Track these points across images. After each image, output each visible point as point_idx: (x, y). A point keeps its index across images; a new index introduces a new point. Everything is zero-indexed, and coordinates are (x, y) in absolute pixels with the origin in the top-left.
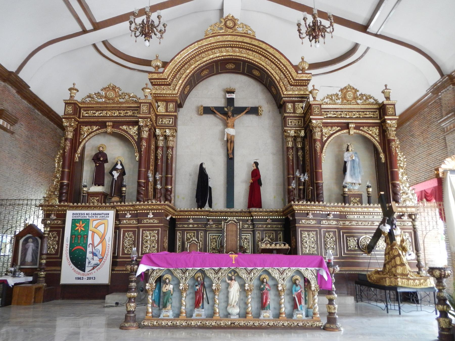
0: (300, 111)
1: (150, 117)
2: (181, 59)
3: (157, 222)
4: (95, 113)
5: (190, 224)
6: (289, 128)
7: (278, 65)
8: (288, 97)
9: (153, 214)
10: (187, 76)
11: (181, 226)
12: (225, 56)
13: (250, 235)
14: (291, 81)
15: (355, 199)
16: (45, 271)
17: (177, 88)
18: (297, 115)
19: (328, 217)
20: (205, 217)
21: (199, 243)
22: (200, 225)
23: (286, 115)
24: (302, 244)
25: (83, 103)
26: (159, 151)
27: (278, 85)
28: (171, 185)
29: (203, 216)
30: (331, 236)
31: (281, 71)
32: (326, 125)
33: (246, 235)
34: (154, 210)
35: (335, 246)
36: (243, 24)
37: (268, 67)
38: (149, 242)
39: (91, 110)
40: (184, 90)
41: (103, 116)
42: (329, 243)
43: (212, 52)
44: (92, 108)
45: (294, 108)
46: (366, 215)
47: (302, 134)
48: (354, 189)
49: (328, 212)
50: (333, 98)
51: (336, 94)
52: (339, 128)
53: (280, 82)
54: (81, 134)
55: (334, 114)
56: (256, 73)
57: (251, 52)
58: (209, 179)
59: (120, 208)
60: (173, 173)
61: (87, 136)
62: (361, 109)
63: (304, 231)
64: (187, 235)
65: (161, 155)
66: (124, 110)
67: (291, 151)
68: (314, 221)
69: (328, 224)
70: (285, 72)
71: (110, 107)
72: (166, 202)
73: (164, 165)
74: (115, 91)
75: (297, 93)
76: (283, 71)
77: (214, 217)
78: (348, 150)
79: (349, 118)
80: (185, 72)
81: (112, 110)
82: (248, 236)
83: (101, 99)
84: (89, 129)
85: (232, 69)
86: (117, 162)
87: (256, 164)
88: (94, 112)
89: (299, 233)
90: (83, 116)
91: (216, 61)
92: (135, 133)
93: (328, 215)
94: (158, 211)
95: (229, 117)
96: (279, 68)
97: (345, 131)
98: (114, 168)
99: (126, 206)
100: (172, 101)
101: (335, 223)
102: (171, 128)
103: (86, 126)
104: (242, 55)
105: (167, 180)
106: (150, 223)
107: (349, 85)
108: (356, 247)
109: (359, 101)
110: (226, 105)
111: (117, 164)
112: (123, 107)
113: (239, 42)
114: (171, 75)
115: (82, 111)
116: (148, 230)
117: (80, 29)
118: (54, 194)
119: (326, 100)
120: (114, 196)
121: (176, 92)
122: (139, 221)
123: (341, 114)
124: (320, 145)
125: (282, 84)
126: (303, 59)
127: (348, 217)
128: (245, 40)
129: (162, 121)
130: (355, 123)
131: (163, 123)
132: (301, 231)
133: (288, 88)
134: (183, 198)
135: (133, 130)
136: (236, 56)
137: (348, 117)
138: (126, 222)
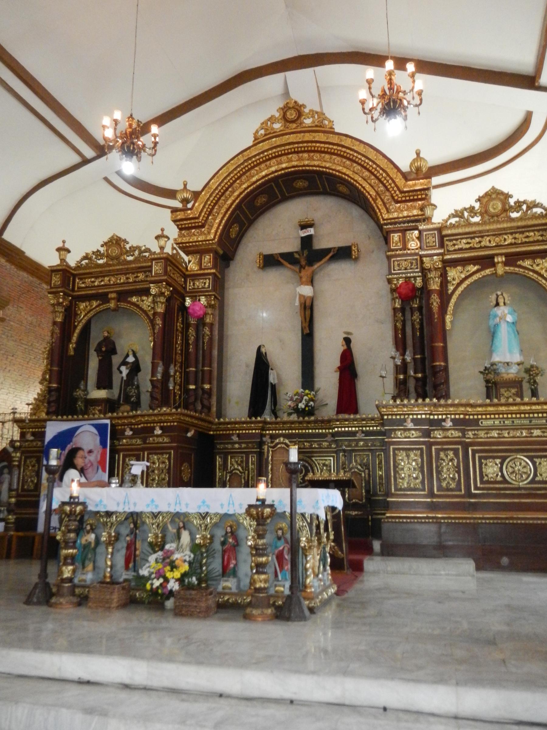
1: (166, 279)
2: (218, 183)
3: (168, 441)
4: (94, 282)
5: (236, 443)
6: (395, 276)
7: (373, 170)
8: (391, 224)
9: (161, 428)
10: (228, 210)
11: (222, 446)
12: (287, 168)
13: (332, 459)
14: (397, 195)
15: (508, 390)
16: (15, 514)
17: (213, 231)
18: (409, 252)
19: (443, 424)
20: (257, 431)
21: (244, 473)
22: (250, 445)
23: (390, 253)
24: (395, 472)
25: (79, 267)
27: (374, 205)
28: (210, 383)
29: (255, 429)
30: (449, 457)
31: (380, 180)
33: (326, 460)
34: (164, 422)
35: (457, 475)
36: (313, 111)
37: (357, 177)
38: (156, 472)
39: (89, 278)
40: (229, 231)
41: (105, 285)
42: (445, 470)
43: (266, 165)
44: (90, 275)
45: (404, 242)
46: (516, 418)
47: (419, 283)
48: (508, 374)
49: (444, 417)
50: (466, 214)
51: (470, 208)
52: (476, 268)
53: (377, 199)
54: (76, 315)
55: (468, 243)
56: (342, 189)
57: (327, 156)
58: (270, 371)
59: (117, 421)
60: (215, 365)
61: (84, 317)
62: (518, 227)
63: (399, 449)
64: (231, 461)
65: (193, 337)
66: (133, 273)
68: (417, 432)
69: (445, 437)
70: (385, 182)
71: (113, 270)
72: (179, 410)
74: (121, 246)
75: (405, 213)
76: (383, 179)
77: (274, 432)
79: (496, 246)
80: (225, 203)
81: (117, 275)
82: (329, 461)
83: (102, 259)
84: (87, 307)
85: (305, 189)
86: (128, 351)
87: (347, 341)
88: (93, 279)
89: (392, 453)
90: (78, 288)
91: (272, 178)
92: (149, 306)
93: (444, 420)
94: (169, 424)
95: (302, 267)
96: (375, 176)
97: (488, 271)
98: (124, 363)
99: (125, 418)
100: (207, 251)
101: (457, 434)
102: (207, 294)
103: (83, 302)
104: (313, 163)
106: (158, 443)
107: (493, 188)
108: (497, 475)
109: (514, 215)
110: (300, 246)
111: (128, 356)
112: (133, 268)
113: (308, 142)
114: (205, 210)
115: (77, 280)
116: (156, 454)
117: (77, 159)
118: (43, 404)
119: (453, 221)
120: (123, 405)
121: (212, 236)
122: (144, 441)
123: (480, 242)
124: (438, 300)
125: (380, 203)
126: (418, 154)
127: (482, 423)
128: (317, 137)
129: (194, 284)
130: (507, 255)
131: (196, 287)
132: (394, 450)
133: (391, 207)
134: (237, 403)
135: (146, 302)
136: (304, 166)
137: (494, 245)
138: (127, 442)
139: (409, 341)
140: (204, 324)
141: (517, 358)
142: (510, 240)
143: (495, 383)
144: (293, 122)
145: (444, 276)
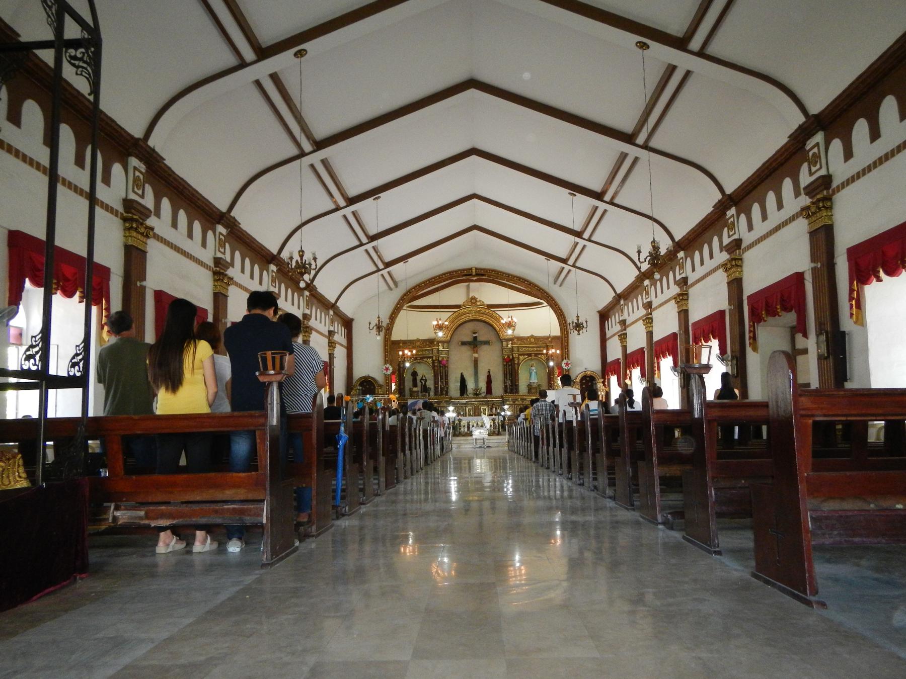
0: (510, 346)
26: (441, 368)
32: (520, 355)
45: (507, 345)
73: (444, 375)
87: (489, 372)
95: (474, 347)
97: (530, 358)
101: (521, 402)
105: (447, 383)
140: (445, 367)
141: (536, 381)
143: (531, 388)
144: (474, 303)
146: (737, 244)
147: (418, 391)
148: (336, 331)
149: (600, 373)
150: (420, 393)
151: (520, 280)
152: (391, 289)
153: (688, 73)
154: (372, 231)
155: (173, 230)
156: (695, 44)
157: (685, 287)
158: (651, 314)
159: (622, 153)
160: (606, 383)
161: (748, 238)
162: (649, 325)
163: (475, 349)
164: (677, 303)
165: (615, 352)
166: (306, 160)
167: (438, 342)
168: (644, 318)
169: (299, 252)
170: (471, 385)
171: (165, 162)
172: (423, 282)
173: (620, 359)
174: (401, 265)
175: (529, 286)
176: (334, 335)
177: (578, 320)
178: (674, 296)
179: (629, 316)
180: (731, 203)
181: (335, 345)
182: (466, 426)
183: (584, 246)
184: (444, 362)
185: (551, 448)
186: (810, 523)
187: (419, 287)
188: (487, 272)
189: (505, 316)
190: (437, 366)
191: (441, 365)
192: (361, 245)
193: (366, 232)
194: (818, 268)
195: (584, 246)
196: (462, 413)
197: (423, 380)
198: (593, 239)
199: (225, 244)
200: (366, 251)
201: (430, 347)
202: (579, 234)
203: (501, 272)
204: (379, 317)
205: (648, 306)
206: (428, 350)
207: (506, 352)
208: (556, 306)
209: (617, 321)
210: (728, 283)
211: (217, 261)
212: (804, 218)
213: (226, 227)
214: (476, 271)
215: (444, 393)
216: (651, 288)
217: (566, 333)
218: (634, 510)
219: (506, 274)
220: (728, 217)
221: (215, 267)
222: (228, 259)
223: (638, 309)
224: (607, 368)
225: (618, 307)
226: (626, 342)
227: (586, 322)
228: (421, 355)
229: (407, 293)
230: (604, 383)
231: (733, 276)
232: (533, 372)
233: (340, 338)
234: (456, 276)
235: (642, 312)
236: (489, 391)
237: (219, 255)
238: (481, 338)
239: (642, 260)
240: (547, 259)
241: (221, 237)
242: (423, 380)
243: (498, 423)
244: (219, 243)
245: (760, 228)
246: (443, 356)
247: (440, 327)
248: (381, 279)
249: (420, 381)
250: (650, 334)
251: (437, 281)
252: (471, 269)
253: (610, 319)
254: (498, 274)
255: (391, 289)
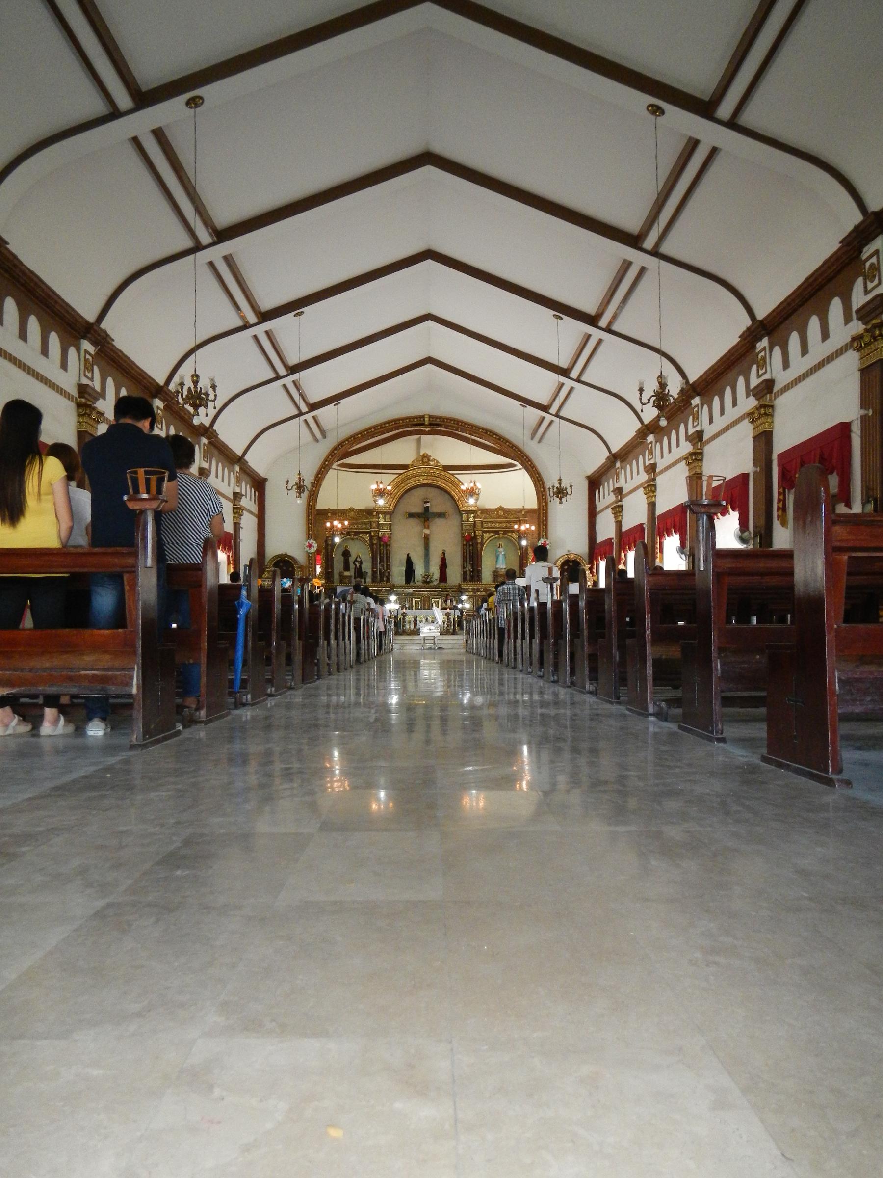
0: (472, 520)
26: (382, 547)
32: (486, 532)
45: (468, 518)
47: (473, 535)
52: (493, 534)
67: (465, 547)
78: (499, 547)
87: (444, 553)
95: (425, 521)
105: (389, 567)
120: (358, 577)
139: (468, 556)
140: (387, 545)
141: (504, 567)
142: (504, 525)
144: (426, 463)
145: (482, 536)
146: (769, 385)
147: (350, 577)
148: (244, 493)
149: (586, 557)
150: (353, 579)
151: (486, 433)
152: (317, 441)
153: (714, 151)
154: (293, 361)
155: (21, 342)
156: (725, 110)
157: (699, 443)
158: (654, 480)
159: (625, 261)
160: (594, 571)
161: (782, 378)
162: (652, 494)
163: (426, 524)
164: (688, 464)
165: (606, 530)
166: (203, 256)
167: (378, 513)
168: (646, 485)
169: (193, 376)
170: (419, 571)
171: (8, 246)
172: (360, 433)
173: (612, 539)
174: (331, 407)
175: (499, 441)
176: (241, 499)
177: (560, 484)
178: (686, 455)
179: (626, 482)
180: (763, 332)
181: (242, 512)
182: (412, 622)
183: (572, 389)
184: (386, 539)
185: (519, 641)
186: (837, 685)
187: (354, 439)
188: (444, 421)
189: (466, 481)
190: (376, 544)
191: (382, 543)
192: (278, 378)
193: (285, 361)
194: (869, 417)
195: (572, 389)
196: (407, 606)
197: (357, 561)
198: (583, 379)
199: (93, 367)
200: (285, 386)
201: (367, 518)
202: (565, 372)
203: (462, 422)
204: (300, 474)
205: (652, 469)
206: (365, 523)
207: (466, 528)
208: (532, 468)
209: (611, 489)
210: (755, 438)
211: (83, 390)
212: (854, 350)
213: (94, 343)
214: (429, 420)
215: (385, 579)
216: (656, 445)
217: (544, 504)
218: (619, 703)
219: (469, 425)
220: (757, 351)
221: (80, 397)
222: (97, 387)
223: (638, 473)
224: (595, 550)
225: (613, 471)
226: (622, 516)
227: (571, 487)
228: (356, 529)
229: (339, 446)
230: (591, 569)
231: (761, 429)
232: (501, 555)
233: (248, 502)
234: (403, 425)
235: (644, 477)
236: (443, 577)
237: (85, 381)
238: (434, 509)
239: (644, 400)
240: (523, 406)
241: (88, 356)
242: (357, 561)
243: (454, 619)
244: (85, 364)
245: (799, 364)
246: (384, 532)
247: (381, 493)
248: (303, 425)
249: (354, 563)
250: (652, 506)
251: (378, 431)
252: (423, 417)
253: (601, 487)
254: (458, 424)
255: (317, 441)
